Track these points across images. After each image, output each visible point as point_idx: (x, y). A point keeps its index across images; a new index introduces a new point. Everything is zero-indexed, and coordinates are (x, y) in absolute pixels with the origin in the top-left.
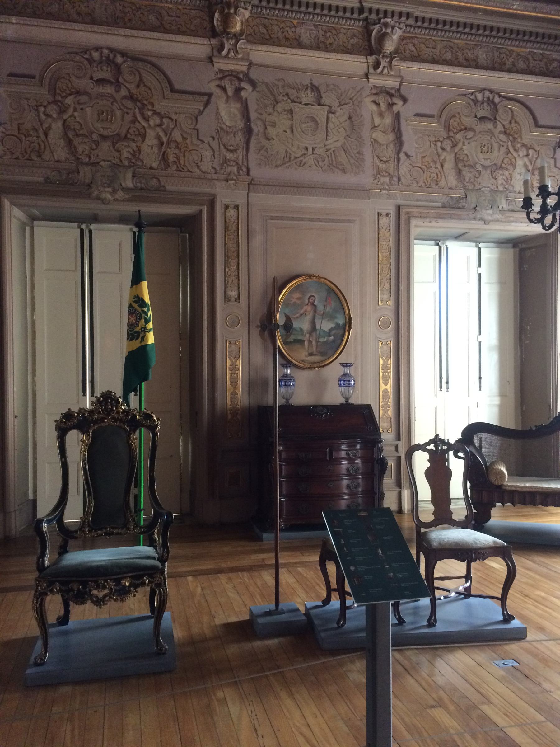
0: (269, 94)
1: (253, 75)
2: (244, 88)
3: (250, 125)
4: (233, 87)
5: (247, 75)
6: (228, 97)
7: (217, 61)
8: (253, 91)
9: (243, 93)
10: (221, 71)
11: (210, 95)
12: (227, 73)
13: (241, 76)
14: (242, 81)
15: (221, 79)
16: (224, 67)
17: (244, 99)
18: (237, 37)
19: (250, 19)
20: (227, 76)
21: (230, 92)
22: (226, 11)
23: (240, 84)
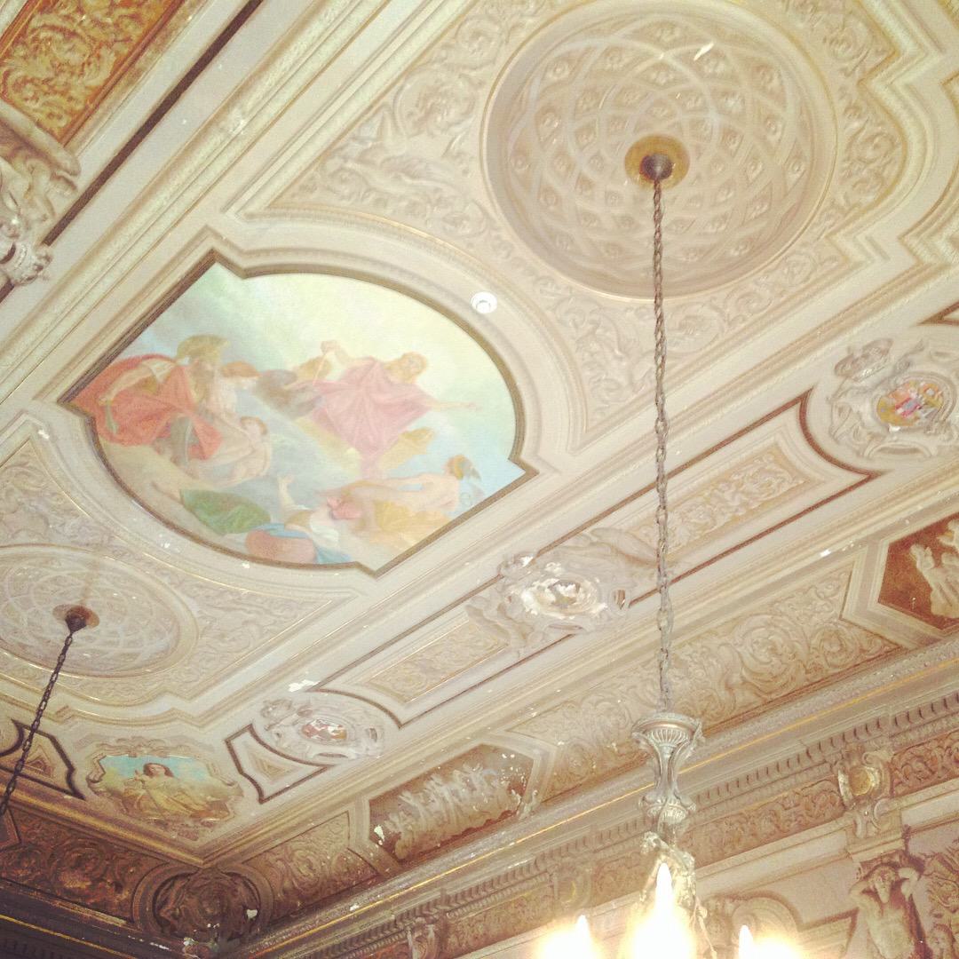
0: (948, 873)
1: (916, 849)
2: (905, 879)
3: (925, 944)
4: (887, 883)
5: (905, 853)
6: (882, 905)
7: (855, 851)
8: (920, 877)
9: (905, 890)
10: (864, 864)
11: (853, 914)
12: (875, 864)
13: (897, 859)
14: (899, 867)
15: (866, 878)
16: (867, 856)
17: (907, 900)
18: (871, 797)
19: (896, 758)
20: (876, 868)
21: (884, 897)
22: (848, 767)
23: (897, 874)
